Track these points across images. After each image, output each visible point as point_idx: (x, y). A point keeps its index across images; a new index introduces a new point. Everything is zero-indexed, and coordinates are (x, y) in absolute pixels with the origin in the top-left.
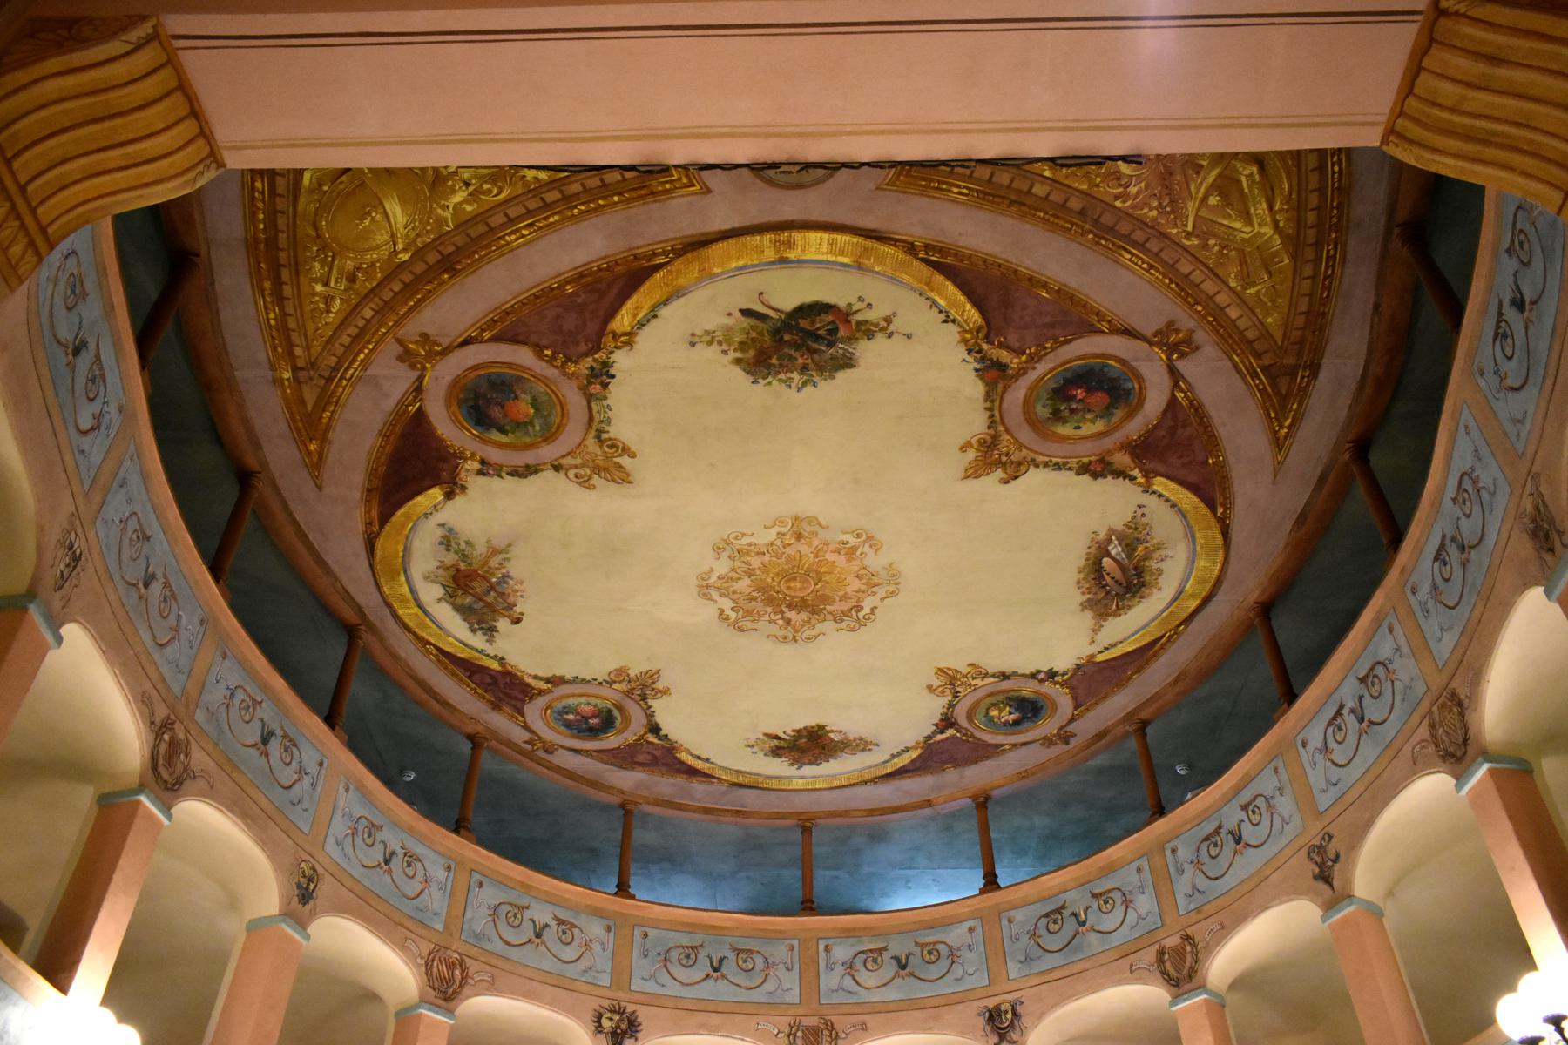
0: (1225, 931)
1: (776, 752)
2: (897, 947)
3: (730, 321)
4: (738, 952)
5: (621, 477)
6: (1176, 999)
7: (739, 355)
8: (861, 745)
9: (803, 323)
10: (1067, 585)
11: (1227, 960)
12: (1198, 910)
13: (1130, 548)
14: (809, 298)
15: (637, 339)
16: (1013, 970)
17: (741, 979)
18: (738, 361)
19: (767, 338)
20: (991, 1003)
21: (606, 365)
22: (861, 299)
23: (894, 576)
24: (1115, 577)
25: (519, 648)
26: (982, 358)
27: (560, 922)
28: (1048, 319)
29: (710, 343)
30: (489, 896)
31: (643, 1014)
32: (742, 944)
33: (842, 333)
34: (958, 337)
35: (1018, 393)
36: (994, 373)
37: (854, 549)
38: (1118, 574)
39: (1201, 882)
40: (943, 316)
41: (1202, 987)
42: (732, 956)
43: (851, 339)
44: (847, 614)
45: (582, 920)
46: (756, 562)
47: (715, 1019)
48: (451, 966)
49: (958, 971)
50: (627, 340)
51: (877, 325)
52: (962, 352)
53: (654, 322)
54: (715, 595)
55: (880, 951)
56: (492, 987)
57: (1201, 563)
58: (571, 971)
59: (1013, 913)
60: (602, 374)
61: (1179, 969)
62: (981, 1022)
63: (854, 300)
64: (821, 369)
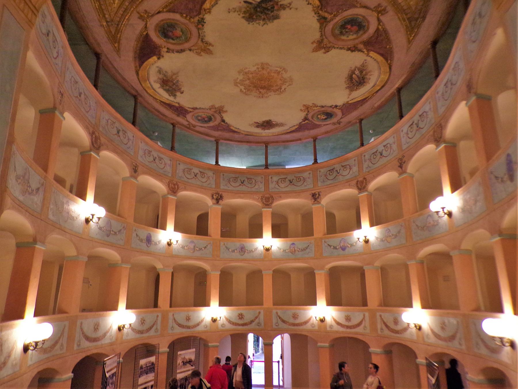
0: (375, 177)
1: (257, 127)
2: (290, 177)
3: (241, 5)
4: (248, 179)
5: (209, 52)
6: (360, 193)
7: (244, 15)
8: (282, 125)
10: (342, 81)
11: (373, 185)
12: (369, 172)
13: (361, 72)
15: (212, 11)
16: (320, 184)
17: (249, 185)
18: (243, 17)
19: (252, 10)
20: (313, 192)
21: (203, 19)
23: (291, 80)
24: (357, 79)
25: (182, 100)
26: (319, 16)
27: (201, 172)
28: (340, 3)
29: (235, 12)
30: (182, 167)
31: (224, 194)
32: (249, 177)
33: (276, 8)
34: (312, 9)
35: (330, 26)
36: (323, 20)
37: (279, 72)
38: (357, 79)
39: (370, 165)
40: (307, 2)
41: (367, 191)
42: (246, 180)
43: (278, 10)
44: (277, 90)
45: (206, 172)
46: (250, 76)
47: (242, 195)
48: (175, 185)
49: (305, 184)
50: (209, 11)
52: (313, 14)
53: (217, 6)
54: (239, 85)
55: (285, 178)
56: (185, 189)
57: (382, 76)
58: (205, 184)
59: (321, 170)
60: (202, 22)
61: (361, 186)
62: (311, 196)
64: (269, 19)
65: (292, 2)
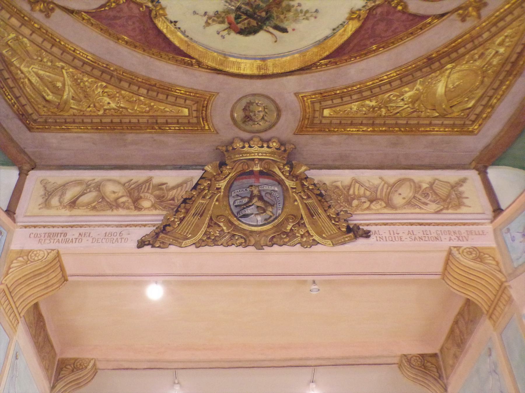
9: (254, 23)
14: (251, 38)
19: (275, 14)
22: (223, 37)
28: (118, 22)
33: (232, 16)
43: (227, 12)
51: (214, 21)
63: (227, 36)
65: (204, 27)
